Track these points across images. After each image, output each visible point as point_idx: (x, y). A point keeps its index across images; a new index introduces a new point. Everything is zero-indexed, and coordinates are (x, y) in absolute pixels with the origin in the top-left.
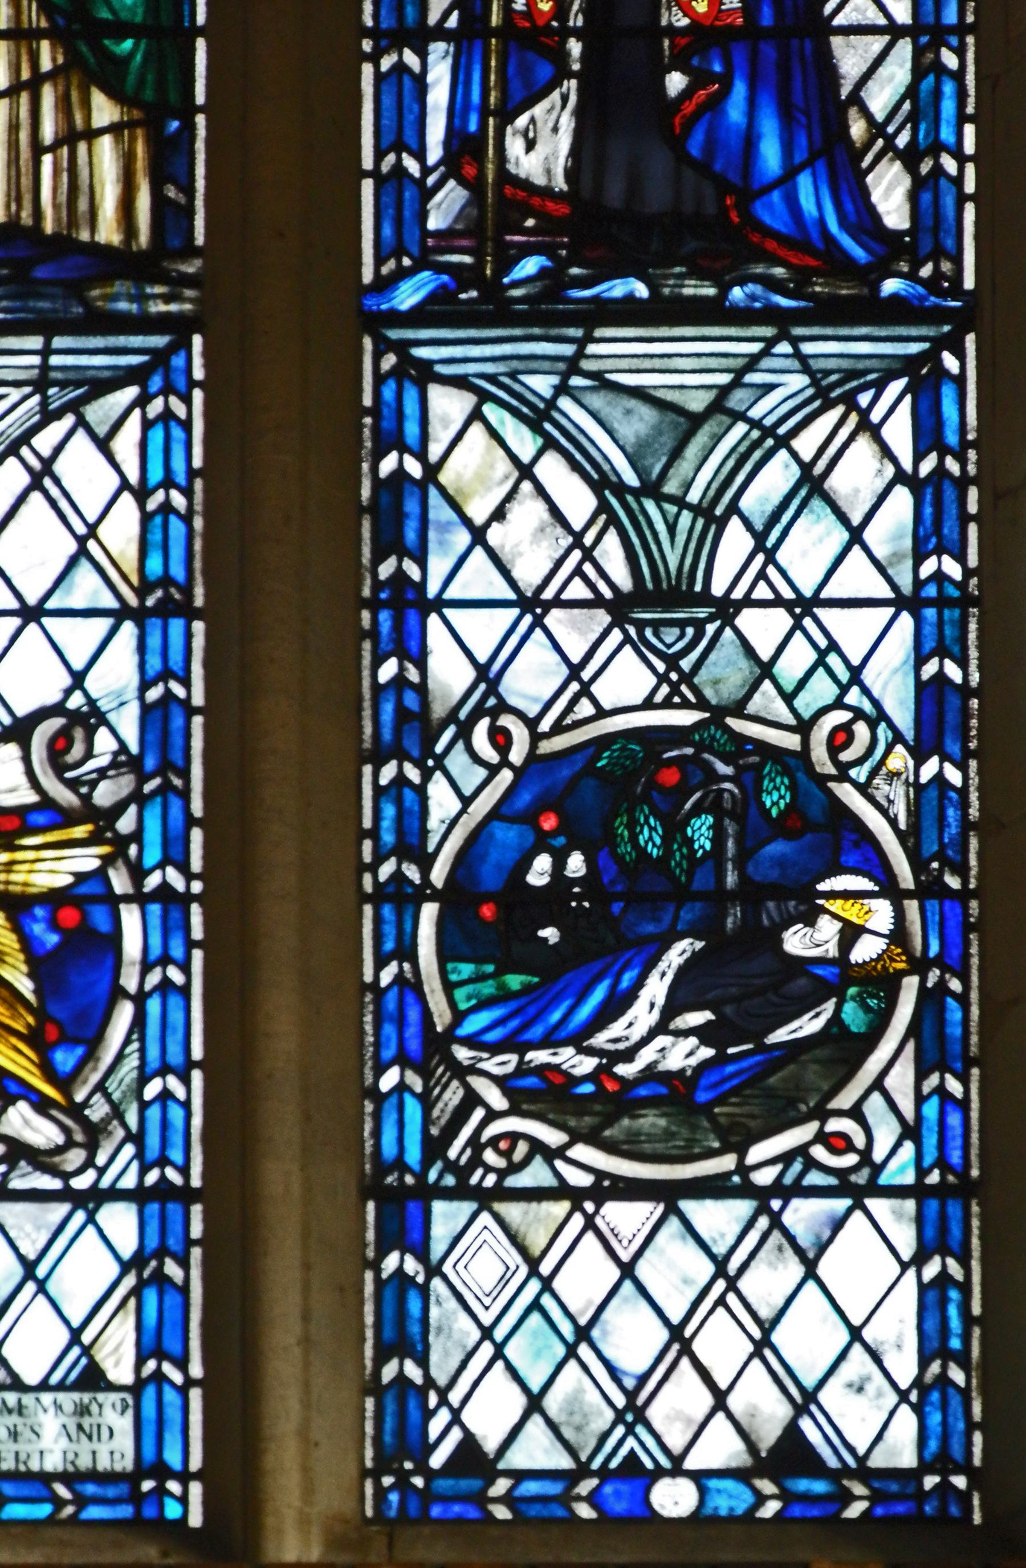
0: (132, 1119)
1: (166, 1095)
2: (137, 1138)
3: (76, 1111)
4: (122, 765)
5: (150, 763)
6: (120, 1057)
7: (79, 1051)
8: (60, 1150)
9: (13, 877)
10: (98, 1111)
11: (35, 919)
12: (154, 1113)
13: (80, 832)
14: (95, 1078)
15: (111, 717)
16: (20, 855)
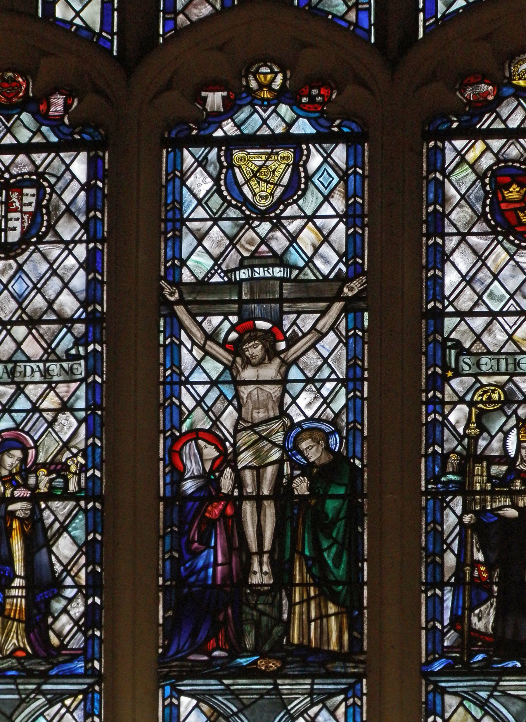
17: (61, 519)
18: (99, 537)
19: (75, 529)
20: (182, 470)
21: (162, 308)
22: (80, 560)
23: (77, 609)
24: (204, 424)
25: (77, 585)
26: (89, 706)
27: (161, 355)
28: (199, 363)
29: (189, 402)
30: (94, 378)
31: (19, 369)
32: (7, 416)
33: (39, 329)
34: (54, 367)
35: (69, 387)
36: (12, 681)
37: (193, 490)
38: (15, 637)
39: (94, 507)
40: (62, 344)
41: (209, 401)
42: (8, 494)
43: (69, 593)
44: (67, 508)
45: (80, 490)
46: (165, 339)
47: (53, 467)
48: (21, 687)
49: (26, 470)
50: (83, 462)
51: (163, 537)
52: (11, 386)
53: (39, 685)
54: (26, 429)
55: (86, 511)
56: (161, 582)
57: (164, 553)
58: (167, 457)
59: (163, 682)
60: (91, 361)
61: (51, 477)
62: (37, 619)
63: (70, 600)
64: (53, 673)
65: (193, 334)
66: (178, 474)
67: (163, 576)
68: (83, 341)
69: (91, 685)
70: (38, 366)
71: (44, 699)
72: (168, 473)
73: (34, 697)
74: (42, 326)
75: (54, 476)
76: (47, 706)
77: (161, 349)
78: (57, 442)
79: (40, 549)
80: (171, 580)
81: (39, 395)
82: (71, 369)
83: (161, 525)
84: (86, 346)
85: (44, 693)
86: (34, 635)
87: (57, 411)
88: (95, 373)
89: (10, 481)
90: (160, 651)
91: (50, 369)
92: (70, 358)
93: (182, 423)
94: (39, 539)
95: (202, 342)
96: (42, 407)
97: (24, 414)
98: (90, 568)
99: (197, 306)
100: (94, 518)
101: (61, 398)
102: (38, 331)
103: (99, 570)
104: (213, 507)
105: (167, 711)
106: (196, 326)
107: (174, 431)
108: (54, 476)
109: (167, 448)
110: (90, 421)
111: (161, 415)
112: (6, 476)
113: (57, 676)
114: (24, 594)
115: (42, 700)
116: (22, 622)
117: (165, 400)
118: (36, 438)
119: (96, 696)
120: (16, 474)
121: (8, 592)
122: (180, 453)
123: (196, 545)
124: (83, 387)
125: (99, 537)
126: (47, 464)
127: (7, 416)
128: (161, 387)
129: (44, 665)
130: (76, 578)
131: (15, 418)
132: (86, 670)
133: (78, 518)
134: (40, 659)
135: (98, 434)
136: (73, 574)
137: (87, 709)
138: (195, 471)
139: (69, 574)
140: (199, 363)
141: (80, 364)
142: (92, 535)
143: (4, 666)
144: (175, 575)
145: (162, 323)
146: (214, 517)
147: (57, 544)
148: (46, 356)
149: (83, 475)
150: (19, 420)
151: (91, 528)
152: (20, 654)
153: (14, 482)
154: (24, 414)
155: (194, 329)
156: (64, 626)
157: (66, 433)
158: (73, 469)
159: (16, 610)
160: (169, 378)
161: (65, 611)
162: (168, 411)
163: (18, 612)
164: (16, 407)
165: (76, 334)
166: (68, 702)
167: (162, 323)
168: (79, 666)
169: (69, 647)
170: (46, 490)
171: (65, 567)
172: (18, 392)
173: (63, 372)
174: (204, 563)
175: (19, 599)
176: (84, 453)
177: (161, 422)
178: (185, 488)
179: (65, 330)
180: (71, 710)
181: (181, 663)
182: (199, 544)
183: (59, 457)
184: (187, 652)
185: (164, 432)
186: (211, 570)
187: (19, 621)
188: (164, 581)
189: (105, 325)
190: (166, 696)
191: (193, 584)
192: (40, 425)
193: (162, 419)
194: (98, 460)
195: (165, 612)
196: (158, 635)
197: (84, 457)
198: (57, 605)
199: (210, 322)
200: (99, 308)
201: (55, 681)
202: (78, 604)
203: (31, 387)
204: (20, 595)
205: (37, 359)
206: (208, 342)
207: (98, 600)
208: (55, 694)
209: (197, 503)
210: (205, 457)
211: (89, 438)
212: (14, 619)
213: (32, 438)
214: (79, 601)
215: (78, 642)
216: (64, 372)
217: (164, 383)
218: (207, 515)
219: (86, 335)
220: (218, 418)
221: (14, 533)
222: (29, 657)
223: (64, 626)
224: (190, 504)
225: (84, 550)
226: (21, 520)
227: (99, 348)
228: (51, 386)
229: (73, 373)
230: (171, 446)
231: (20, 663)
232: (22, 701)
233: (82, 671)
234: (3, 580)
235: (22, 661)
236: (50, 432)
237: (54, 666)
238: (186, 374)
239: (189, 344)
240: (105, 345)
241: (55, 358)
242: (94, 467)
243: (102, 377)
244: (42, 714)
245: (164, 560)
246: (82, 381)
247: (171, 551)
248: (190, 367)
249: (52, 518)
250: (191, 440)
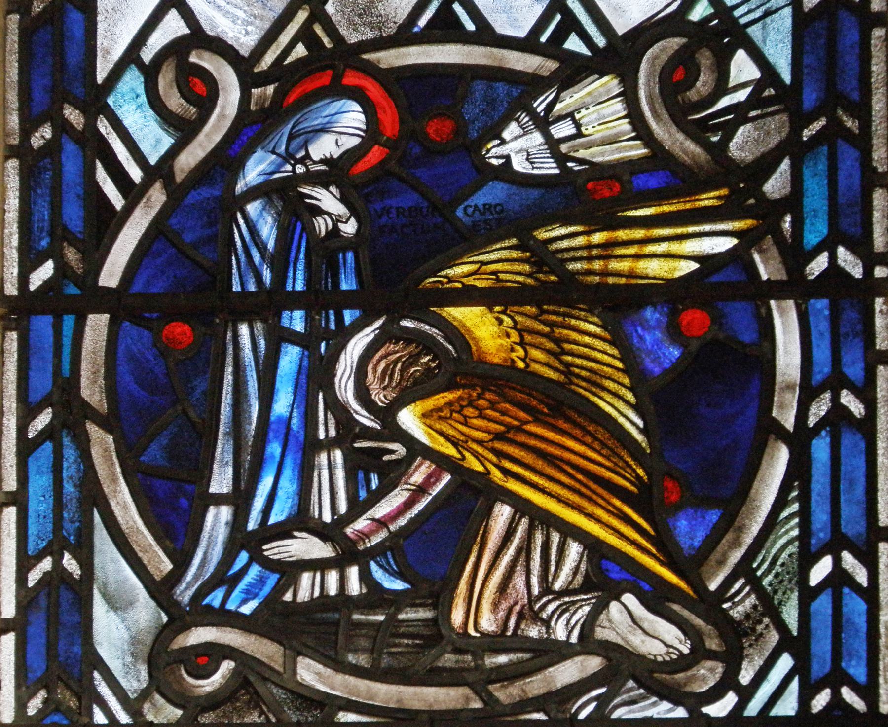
0: (791, 616)
1: (839, 578)
2: (796, 645)
3: (710, 605)
4: (770, 101)
5: (810, 97)
6: (771, 523)
7: (714, 516)
8: (684, 663)
9: (614, 265)
10: (741, 607)
11: (647, 327)
12: (823, 605)
13: (708, 199)
14: (736, 556)
15: (754, 32)
16: (622, 234)
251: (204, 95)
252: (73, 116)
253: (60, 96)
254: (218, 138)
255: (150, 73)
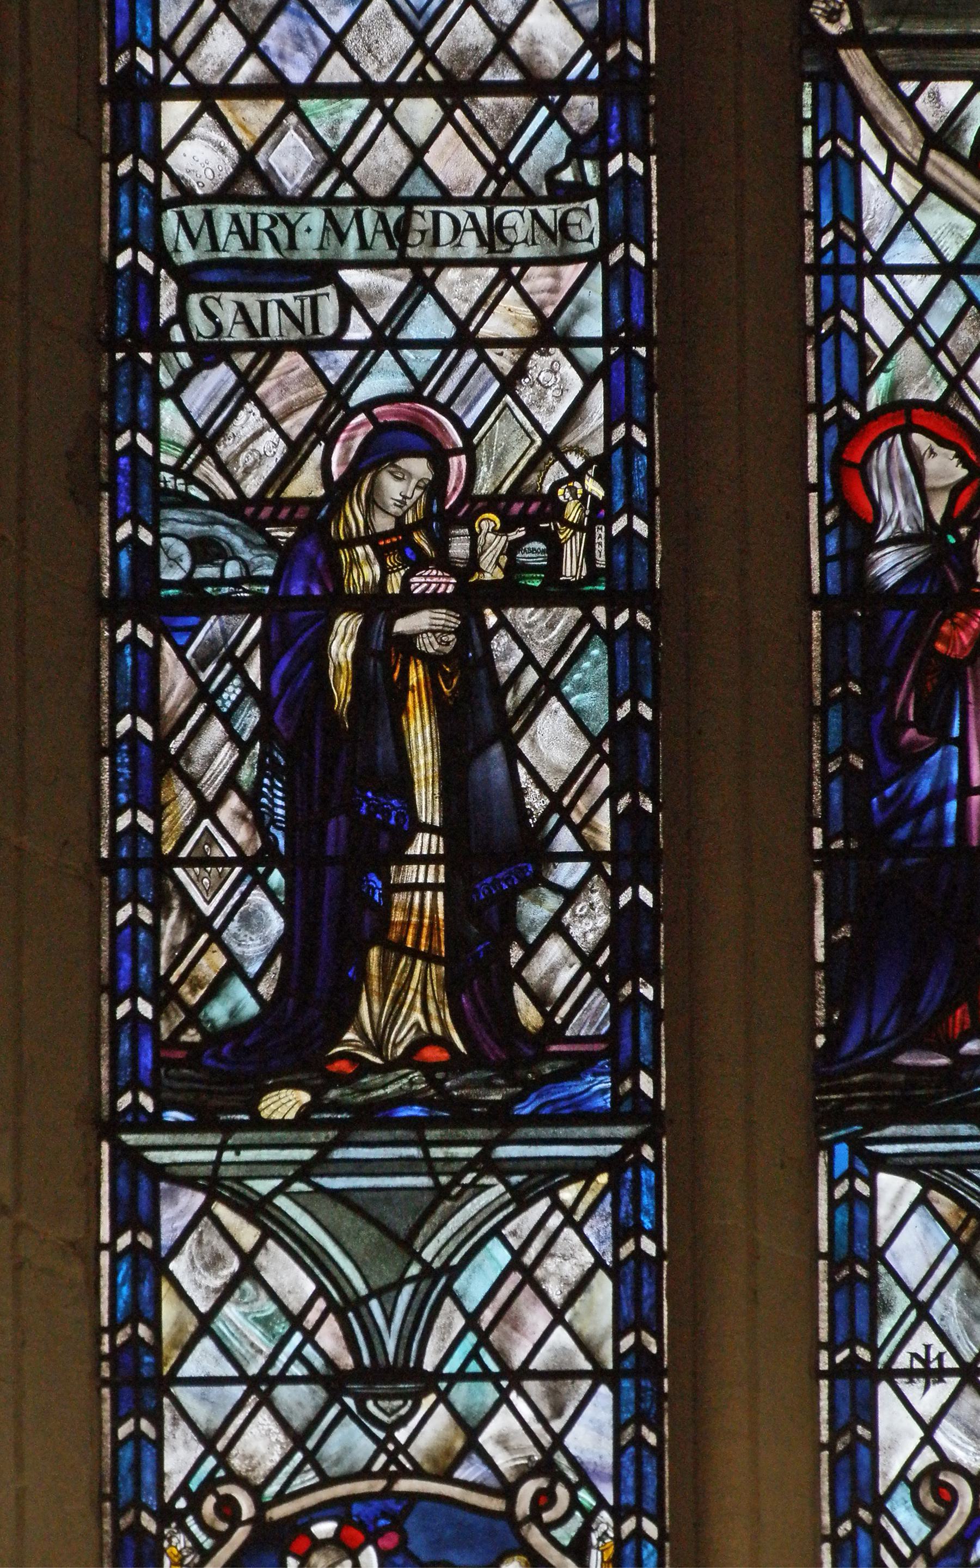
17: (543, 658)
18: (647, 712)
19: (582, 687)
20: (871, 519)
21: (807, 55)
22: (596, 779)
23: (591, 923)
24: (926, 386)
25: (588, 853)
26: (626, 1208)
27: (808, 189)
28: (908, 213)
29: (885, 325)
30: (627, 250)
31: (418, 223)
32: (386, 357)
33: (474, 109)
34: (516, 219)
35: (557, 276)
36: (412, 1135)
37: (900, 575)
38: (418, 1004)
39: (632, 623)
40: (535, 152)
41: (938, 322)
42: (394, 585)
43: (568, 874)
44: (559, 627)
45: (594, 574)
46: (817, 144)
47: (517, 508)
48: (436, 1152)
49: (444, 514)
50: (599, 492)
51: (823, 711)
52: (399, 271)
53: (488, 1146)
54: (442, 397)
55: (609, 636)
56: (818, 843)
57: (826, 758)
58: (828, 480)
59: (828, 1131)
60: (617, 202)
61: (513, 536)
62: (480, 956)
63: (570, 896)
64: (525, 1109)
65: (891, 129)
66: (858, 530)
67: (823, 823)
68: (594, 144)
69: (631, 1145)
70: (472, 216)
71: (501, 1188)
72: (833, 525)
73: (473, 1183)
74: (483, 100)
75: (521, 533)
76: (511, 1208)
77: (807, 172)
78: (528, 435)
79: (482, 748)
80: (846, 837)
81: (475, 298)
82: (563, 223)
83: (817, 678)
84: (603, 159)
85: (501, 1170)
86: (473, 1000)
87: (527, 346)
88: (628, 240)
89: (398, 548)
90: (820, 1040)
91: (506, 223)
92: (559, 192)
93: (866, 383)
94: (481, 718)
95: (917, 154)
96: (485, 332)
97: (434, 354)
98: (624, 802)
99: (899, 51)
100: (633, 656)
101: (536, 309)
102: (470, 115)
103: (649, 807)
104: (953, 624)
105: (842, 1217)
106: (898, 108)
107: (845, 405)
108: (521, 533)
109: (828, 455)
110: (618, 377)
111: (811, 360)
112: (386, 535)
113: (535, 1119)
114: (442, 879)
115: (496, 1191)
116: (439, 961)
117: (820, 317)
118: (469, 422)
119: (647, 1176)
120: (416, 526)
121: (398, 872)
122: (863, 469)
123: (911, 733)
124: (597, 276)
125: (647, 712)
126: (502, 497)
127: (386, 357)
128: (809, 280)
129: (500, 1087)
130: (586, 832)
131: (412, 365)
132: (617, 1099)
133: (589, 657)
134: (488, 1067)
135: (640, 414)
136: (576, 818)
137: (623, 1215)
138: (904, 522)
139: (566, 820)
140: (908, 213)
141: (587, 211)
142: (627, 705)
143: (389, 1090)
144: (856, 821)
145: (807, 98)
146: (957, 653)
147: (530, 732)
148: (493, 185)
149: (600, 532)
150: (420, 370)
151: (623, 686)
152: (433, 1054)
153: (409, 552)
154: (434, 354)
155: (894, 117)
156: (554, 970)
157: (551, 411)
158: (573, 512)
159: (420, 926)
160: (831, 254)
161: (556, 926)
162: (828, 347)
163: (425, 931)
164: (413, 331)
165: (574, 125)
166: (567, 1195)
167: (807, 98)
168: (597, 1087)
169: (568, 1033)
170: (500, 575)
171: (555, 798)
172: (419, 289)
173: (539, 232)
174: (934, 786)
175: (429, 894)
176: (601, 466)
177: (811, 380)
178: (877, 570)
179: (544, 112)
180: (577, 1217)
181: (879, 1076)
182: (921, 732)
183: (534, 478)
184: (892, 1043)
185: (819, 408)
186: (952, 807)
187: (429, 958)
188: (827, 840)
189: (652, 100)
190: (838, 1173)
191: (905, 848)
192: (481, 385)
193: (812, 371)
194: (640, 490)
195: (830, 928)
196: (814, 994)
197: (603, 478)
198: (536, 911)
199: (936, 97)
200: (636, 51)
201: (532, 1133)
202: (592, 906)
203: (452, 274)
204: (431, 880)
205: (470, 193)
206: (933, 155)
207: (646, 896)
208: (531, 1173)
209: (912, 614)
210: (929, 483)
211: (616, 425)
212: (415, 954)
213: (457, 422)
214: (596, 897)
215: (592, 1017)
216: (543, 234)
217: (817, 269)
218: (940, 646)
219: (600, 127)
220: (964, 371)
221: (411, 700)
222: (456, 1064)
223: (554, 970)
224: (891, 619)
225: (606, 748)
226: (432, 663)
227: (637, 165)
228: (509, 273)
229: (567, 237)
230: (838, 451)
231: (431, 1081)
232: (441, 1193)
233: (605, 1102)
234: (385, 839)
235: (439, 1075)
236: (506, 405)
237: (529, 1089)
238: (876, 242)
239: (880, 159)
240: (653, 158)
241: (518, 193)
242: (630, 510)
243: (647, 250)
244: (496, 1232)
245: (827, 779)
246: (591, 259)
247: (843, 752)
248: (884, 224)
249: (519, 654)
250: (892, 433)
251: (949, 1500)
252: (864, 1514)
253: (856, 1503)
254: (959, 1526)
255: (914, 1487)
